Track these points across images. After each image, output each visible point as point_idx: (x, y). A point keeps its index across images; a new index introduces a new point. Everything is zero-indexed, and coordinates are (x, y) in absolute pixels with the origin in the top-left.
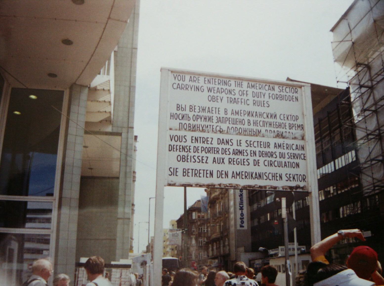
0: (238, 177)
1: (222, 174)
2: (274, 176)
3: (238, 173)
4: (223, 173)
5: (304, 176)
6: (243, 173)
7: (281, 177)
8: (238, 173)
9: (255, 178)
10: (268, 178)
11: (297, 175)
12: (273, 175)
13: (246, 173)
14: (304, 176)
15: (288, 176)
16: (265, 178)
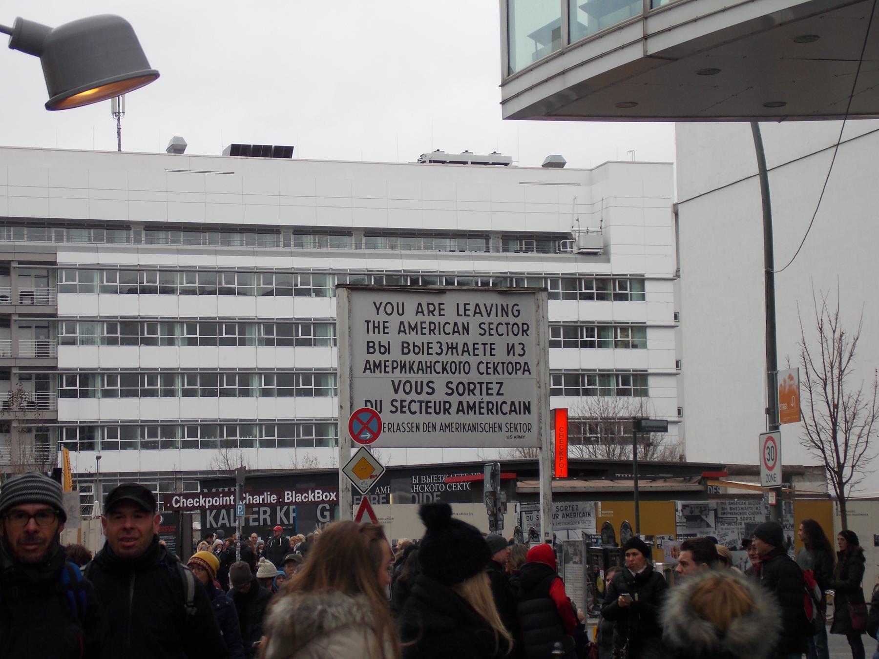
4: (431, 425)
6: (454, 425)
7: (500, 428)
10: (484, 429)
15: (508, 426)
16: (480, 429)
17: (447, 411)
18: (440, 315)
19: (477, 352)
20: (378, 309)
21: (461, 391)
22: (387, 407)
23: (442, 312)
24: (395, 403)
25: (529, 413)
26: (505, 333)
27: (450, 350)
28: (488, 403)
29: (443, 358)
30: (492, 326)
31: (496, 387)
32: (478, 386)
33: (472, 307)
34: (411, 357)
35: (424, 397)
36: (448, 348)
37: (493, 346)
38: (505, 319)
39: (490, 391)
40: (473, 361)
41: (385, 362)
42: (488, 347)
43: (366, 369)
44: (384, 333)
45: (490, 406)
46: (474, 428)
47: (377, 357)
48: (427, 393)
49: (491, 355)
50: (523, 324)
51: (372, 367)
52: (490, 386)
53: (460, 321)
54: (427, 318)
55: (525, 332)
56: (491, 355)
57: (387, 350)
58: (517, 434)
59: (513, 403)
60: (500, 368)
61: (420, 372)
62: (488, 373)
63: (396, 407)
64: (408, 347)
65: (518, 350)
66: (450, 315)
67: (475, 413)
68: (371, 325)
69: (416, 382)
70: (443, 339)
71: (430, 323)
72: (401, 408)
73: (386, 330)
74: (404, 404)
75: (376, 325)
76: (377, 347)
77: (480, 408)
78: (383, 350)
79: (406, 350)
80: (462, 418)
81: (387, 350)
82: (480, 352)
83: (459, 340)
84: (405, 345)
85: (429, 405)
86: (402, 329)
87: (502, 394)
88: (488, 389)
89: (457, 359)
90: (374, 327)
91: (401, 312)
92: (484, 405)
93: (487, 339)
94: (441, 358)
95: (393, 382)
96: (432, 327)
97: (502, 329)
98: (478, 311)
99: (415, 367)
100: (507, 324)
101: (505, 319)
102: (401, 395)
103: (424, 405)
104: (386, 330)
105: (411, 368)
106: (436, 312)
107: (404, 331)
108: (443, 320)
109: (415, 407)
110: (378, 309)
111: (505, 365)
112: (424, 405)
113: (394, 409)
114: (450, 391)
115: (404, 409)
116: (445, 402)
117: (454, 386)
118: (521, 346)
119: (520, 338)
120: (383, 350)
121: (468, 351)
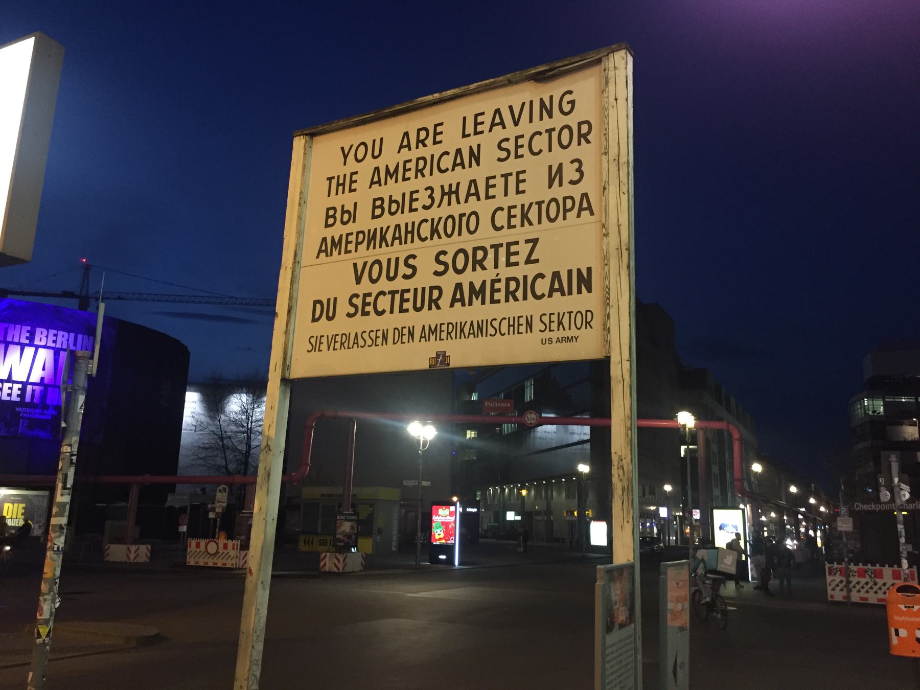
0: (432, 337)
1: (403, 335)
2: (513, 326)
3: (433, 329)
4: (406, 331)
5: (589, 314)
6: (444, 328)
7: (529, 325)
8: (433, 329)
9: (469, 333)
10: (498, 331)
11: (570, 313)
12: (511, 323)
13: (450, 326)
14: (589, 314)
15: (546, 319)
17: (435, 303)
18: (435, 143)
19: (492, 192)
20: (345, 157)
21: (460, 266)
22: (344, 307)
23: (438, 138)
24: (355, 300)
25: (589, 290)
26: (545, 148)
27: (446, 198)
28: (508, 280)
29: (434, 213)
30: (520, 142)
31: (524, 249)
32: (491, 252)
33: (487, 119)
34: (387, 221)
35: (399, 284)
36: (443, 194)
37: (522, 177)
38: (547, 123)
39: (513, 259)
40: (484, 208)
41: (348, 235)
42: (512, 180)
43: (320, 251)
44: (351, 190)
45: (513, 285)
46: (479, 329)
47: (339, 230)
48: (405, 277)
49: (518, 192)
50: (580, 124)
51: (329, 247)
52: (513, 249)
53: (465, 145)
54: (414, 154)
55: (584, 137)
56: (518, 192)
57: (351, 215)
58: (562, 333)
59: (556, 275)
60: (533, 215)
61: (397, 242)
62: (510, 226)
63: (356, 307)
64: (381, 207)
65: (570, 173)
66: (452, 140)
67: (483, 303)
68: (334, 182)
69: (389, 260)
70: (438, 180)
71: (418, 159)
72: (362, 306)
73: (354, 186)
74: (368, 300)
75: (341, 181)
76: (338, 215)
77: (494, 291)
78: (346, 217)
79: (378, 212)
80: (460, 314)
81: (351, 215)
82: (498, 191)
83: (462, 176)
84: (378, 203)
85: (406, 296)
86: (376, 179)
87: (537, 261)
88: (509, 254)
89: (456, 210)
90: (338, 185)
91: (376, 153)
92: (501, 285)
93: (513, 165)
94: (428, 214)
95: (355, 265)
96: (421, 163)
97: (540, 143)
98: (497, 120)
99: (389, 237)
100: (550, 131)
101: (547, 123)
102: (366, 286)
103: (398, 297)
104: (354, 186)
105: (383, 238)
106: (429, 142)
107: (379, 182)
108: (437, 150)
109: (384, 303)
110: (345, 157)
111: (544, 206)
112: (398, 297)
113: (352, 310)
114: (441, 268)
115: (367, 309)
116: (432, 289)
117: (448, 259)
118: (576, 165)
119: (575, 151)
120: (346, 217)
121: (477, 194)
